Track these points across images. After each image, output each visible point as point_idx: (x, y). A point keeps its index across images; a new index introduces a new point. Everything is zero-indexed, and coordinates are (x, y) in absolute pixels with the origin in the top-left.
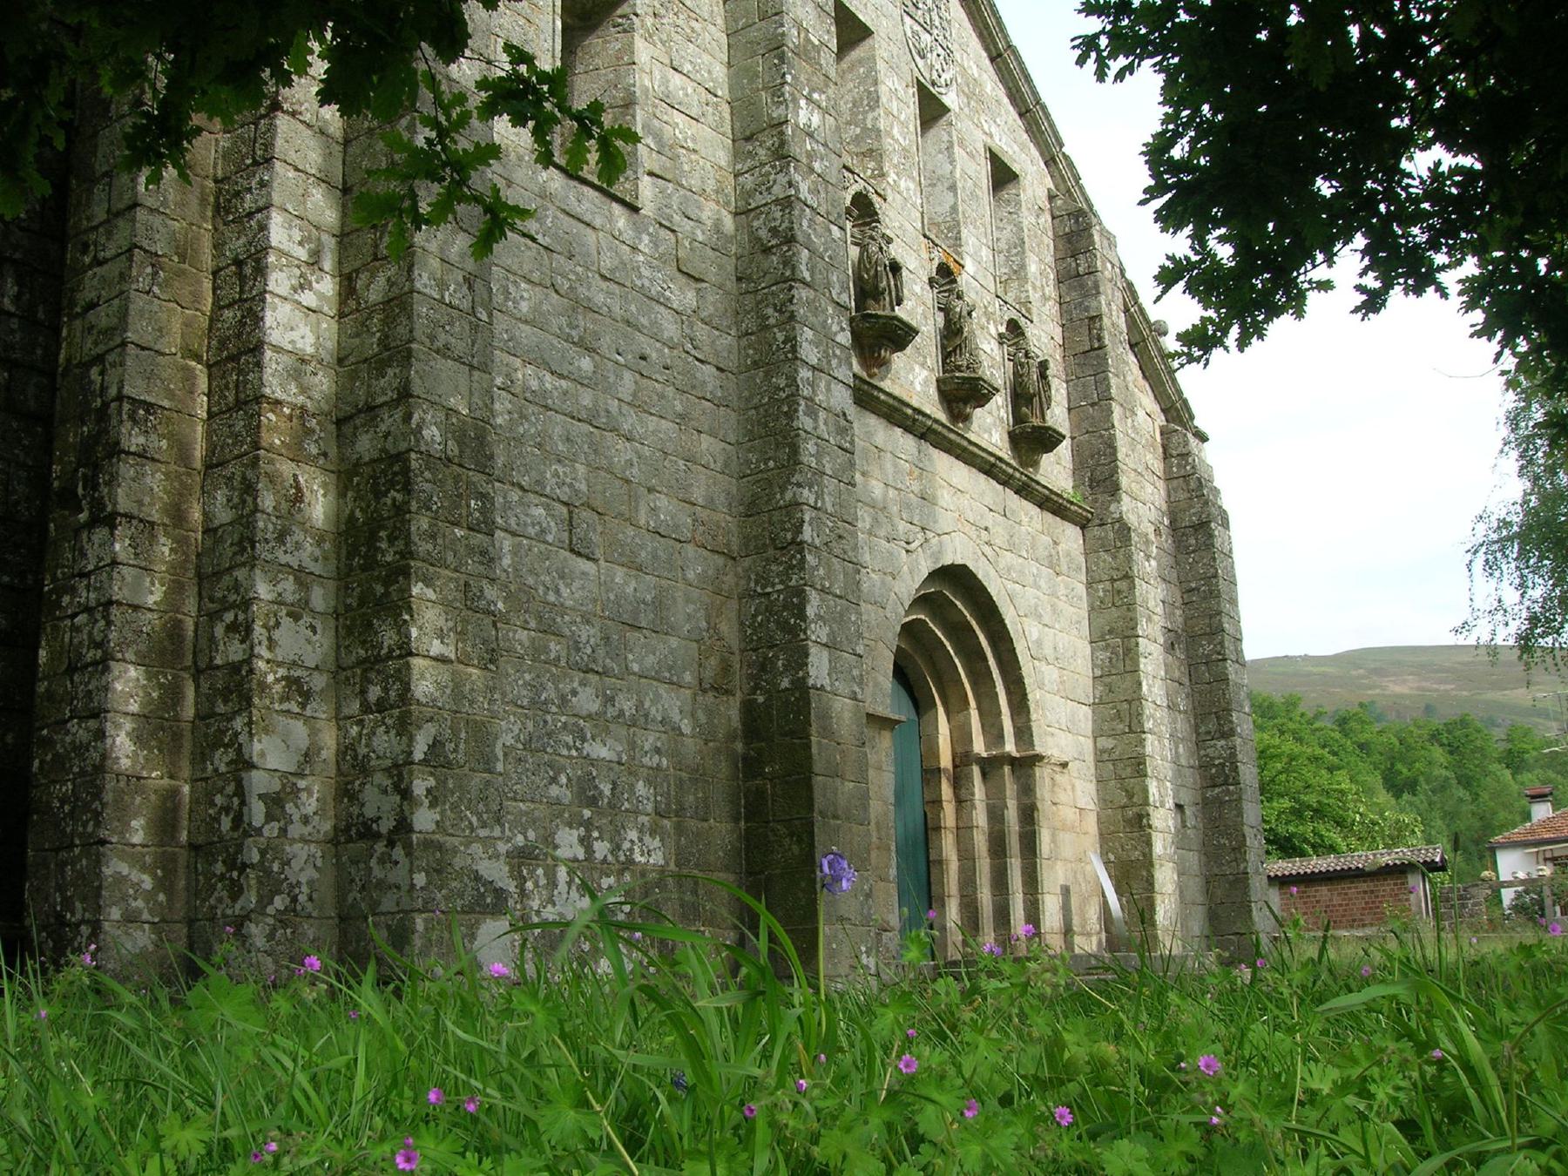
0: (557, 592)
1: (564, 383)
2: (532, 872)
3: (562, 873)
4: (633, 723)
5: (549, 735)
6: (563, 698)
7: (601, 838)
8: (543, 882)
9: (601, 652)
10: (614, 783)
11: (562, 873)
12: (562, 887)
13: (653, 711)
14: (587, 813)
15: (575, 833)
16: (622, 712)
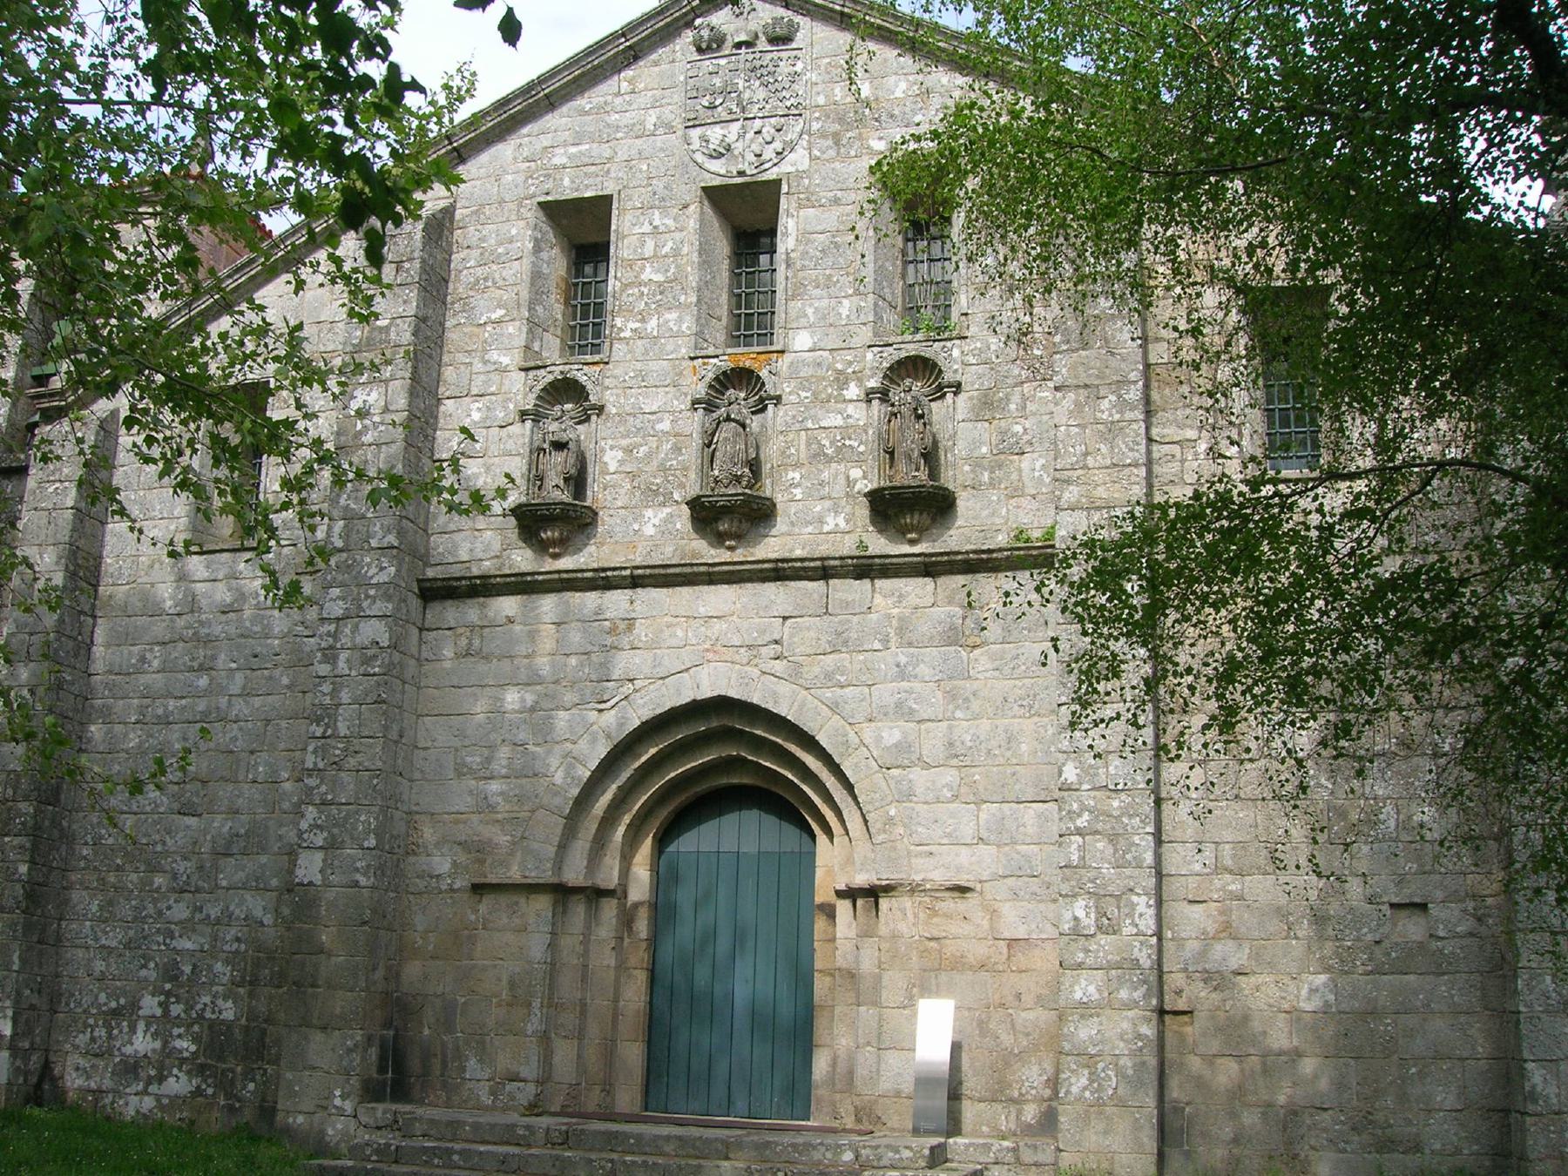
0: (164, 843)
1: (184, 702)
2: (118, 1025)
4: (218, 922)
5: (145, 938)
6: (160, 913)
7: (178, 1002)
8: (126, 1030)
9: (194, 878)
10: (195, 966)
11: (141, 1026)
12: (140, 1034)
13: (237, 912)
14: (168, 986)
15: (156, 999)
16: (208, 916)
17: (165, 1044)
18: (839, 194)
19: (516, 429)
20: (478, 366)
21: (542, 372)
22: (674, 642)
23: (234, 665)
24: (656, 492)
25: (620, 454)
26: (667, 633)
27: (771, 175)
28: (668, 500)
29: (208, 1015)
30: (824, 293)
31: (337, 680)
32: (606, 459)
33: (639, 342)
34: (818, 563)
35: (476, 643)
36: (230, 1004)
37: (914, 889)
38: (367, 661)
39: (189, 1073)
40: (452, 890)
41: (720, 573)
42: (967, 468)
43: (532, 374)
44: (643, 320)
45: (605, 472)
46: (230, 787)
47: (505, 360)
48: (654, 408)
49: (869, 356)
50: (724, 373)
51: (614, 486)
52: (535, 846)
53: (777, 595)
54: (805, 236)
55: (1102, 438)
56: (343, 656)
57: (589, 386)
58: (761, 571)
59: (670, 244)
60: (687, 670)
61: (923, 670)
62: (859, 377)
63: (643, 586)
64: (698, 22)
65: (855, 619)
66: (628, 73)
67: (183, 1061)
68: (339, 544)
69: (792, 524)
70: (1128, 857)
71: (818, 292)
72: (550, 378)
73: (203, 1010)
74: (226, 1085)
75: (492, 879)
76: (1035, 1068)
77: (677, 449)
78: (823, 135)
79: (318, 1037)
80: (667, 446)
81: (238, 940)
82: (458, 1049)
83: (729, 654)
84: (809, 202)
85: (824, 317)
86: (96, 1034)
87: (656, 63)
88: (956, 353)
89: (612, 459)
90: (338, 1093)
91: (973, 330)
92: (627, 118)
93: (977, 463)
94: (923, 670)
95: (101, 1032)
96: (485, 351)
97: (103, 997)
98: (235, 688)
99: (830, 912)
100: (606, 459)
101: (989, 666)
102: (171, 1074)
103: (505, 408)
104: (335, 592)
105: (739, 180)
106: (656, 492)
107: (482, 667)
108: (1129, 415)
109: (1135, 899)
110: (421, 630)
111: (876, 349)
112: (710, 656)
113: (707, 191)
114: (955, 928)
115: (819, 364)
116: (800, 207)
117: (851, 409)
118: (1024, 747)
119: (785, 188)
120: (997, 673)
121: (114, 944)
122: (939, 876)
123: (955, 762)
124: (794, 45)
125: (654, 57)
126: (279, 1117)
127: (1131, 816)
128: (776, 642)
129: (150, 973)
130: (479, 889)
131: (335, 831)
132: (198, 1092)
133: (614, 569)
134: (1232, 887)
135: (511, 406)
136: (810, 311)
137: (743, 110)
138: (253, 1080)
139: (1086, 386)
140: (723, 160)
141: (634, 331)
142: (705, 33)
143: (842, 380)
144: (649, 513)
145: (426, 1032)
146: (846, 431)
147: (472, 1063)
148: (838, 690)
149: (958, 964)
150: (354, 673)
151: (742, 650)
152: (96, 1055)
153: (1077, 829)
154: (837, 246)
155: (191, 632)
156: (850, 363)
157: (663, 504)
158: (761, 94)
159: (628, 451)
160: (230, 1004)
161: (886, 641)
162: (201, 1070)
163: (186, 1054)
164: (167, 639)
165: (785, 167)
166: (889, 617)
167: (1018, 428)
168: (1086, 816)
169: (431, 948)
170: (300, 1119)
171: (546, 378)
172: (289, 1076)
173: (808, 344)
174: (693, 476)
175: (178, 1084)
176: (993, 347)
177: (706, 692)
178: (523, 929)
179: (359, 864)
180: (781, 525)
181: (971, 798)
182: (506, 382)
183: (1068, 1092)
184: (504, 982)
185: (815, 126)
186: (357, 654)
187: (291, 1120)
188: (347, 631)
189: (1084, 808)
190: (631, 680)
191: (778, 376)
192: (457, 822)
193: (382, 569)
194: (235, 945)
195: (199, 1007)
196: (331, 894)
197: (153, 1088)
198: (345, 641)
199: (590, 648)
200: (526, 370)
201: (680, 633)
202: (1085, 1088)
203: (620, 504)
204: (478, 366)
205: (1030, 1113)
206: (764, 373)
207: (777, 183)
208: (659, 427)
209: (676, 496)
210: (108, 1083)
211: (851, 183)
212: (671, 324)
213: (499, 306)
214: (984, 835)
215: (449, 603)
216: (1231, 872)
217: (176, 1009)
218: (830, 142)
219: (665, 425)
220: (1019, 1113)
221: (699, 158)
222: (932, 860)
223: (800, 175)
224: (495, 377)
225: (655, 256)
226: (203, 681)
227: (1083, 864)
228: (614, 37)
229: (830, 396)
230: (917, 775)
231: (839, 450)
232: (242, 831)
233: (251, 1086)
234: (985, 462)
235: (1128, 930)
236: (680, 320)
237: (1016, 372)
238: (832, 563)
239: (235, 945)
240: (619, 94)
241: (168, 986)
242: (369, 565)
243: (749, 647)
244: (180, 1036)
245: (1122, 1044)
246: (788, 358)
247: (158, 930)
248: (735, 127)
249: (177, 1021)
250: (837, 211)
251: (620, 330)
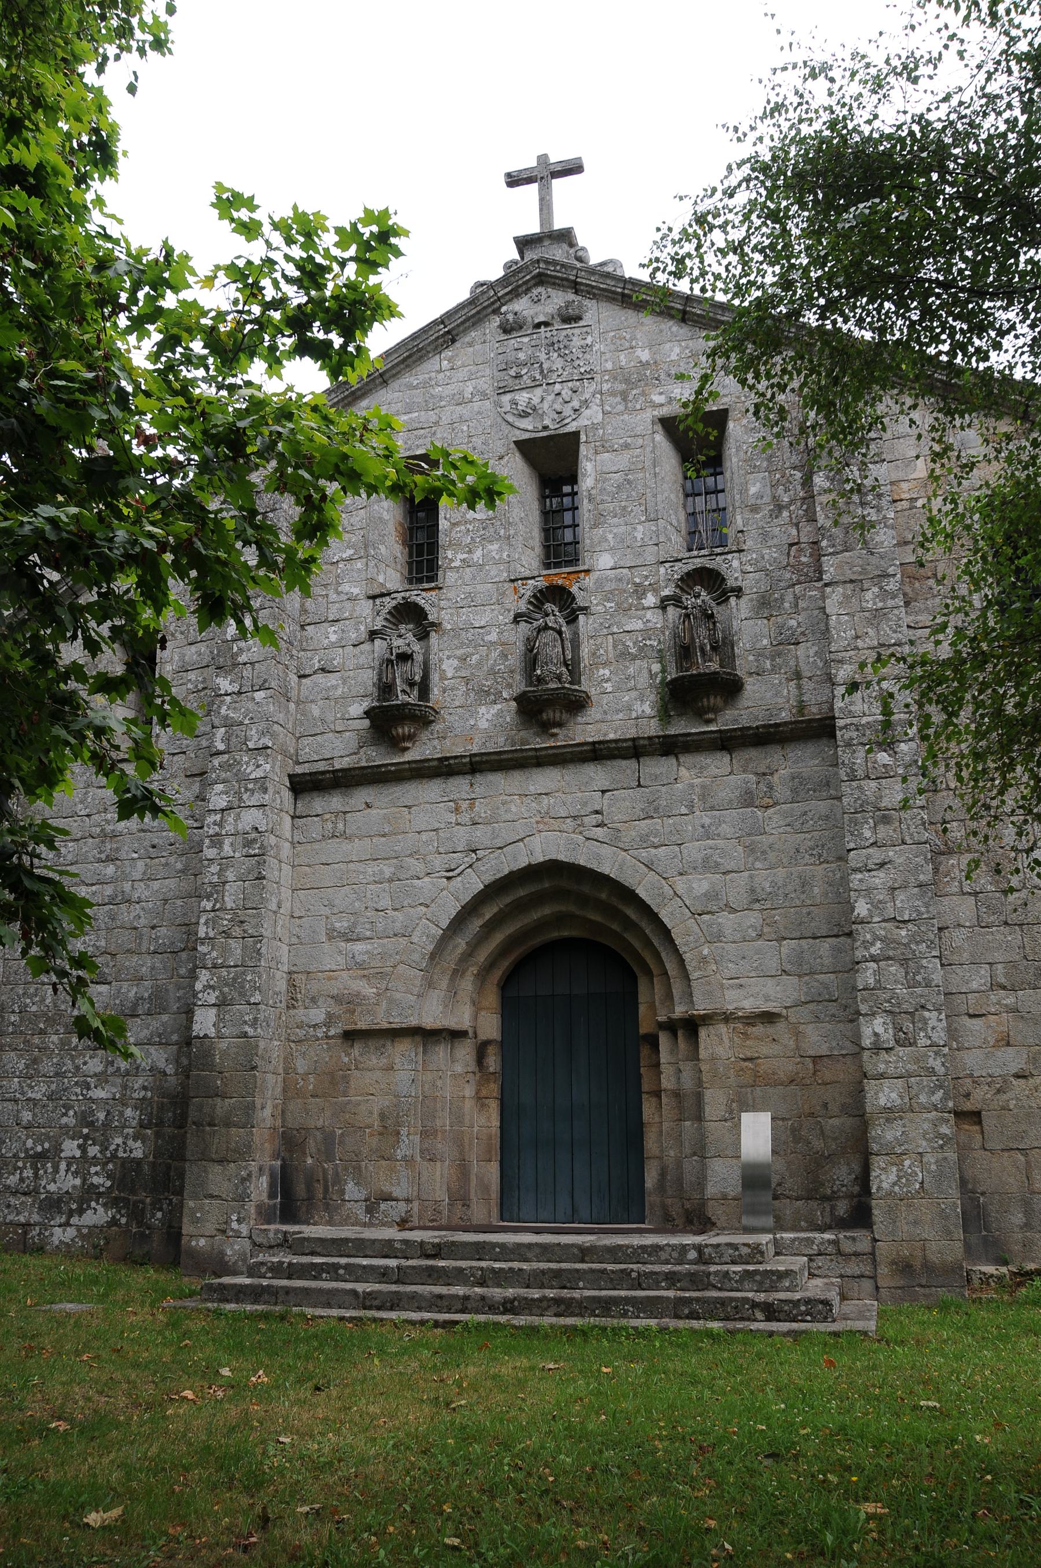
1: (94, 888)
2: (44, 1166)
3: (63, 1166)
4: (127, 1073)
5: (65, 1090)
6: (77, 1068)
7: (94, 1144)
8: (50, 1170)
10: (108, 1113)
11: (63, 1166)
12: (62, 1173)
13: (144, 1064)
14: (85, 1131)
15: (76, 1143)
16: (119, 1069)
17: (84, 1180)
18: (629, 440)
19: (366, 647)
20: (333, 597)
21: (387, 599)
22: (509, 817)
23: (135, 856)
24: (488, 693)
25: (456, 662)
26: (503, 809)
27: (572, 428)
28: (498, 698)
29: (121, 1154)
30: (621, 521)
31: (224, 863)
32: (444, 667)
33: (468, 570)
34: (630, 743)
35: (341, 826)
36: (139, 1144)
37: (727, 1018)
38: (248, 844)
39: (105, 1205)
40: (327, 1037)
41: (546, 756)
42: (751, 658)
43: (378, 601)
44: (470, 552)
45: (443, 678)
46: (135, 958)
47: (356, 591)
48: (482, 623)
49: (662, 570)
50: (541, 591)
51: (452, 689)
52: (398, 996)
53: (597, 775)
54: (602, 476)
55: (869, 622)
56: (227, 842)
57: (427, 608)
58: (581, 752)
60: (522, 840)
61: (725, 829)
62: (654, 588)
63: (481, 771)
64: (504, 309)
65: (664, 789)
66: (447, 353)
67: (100, 1195)
68: (221, 747)
69: (605, 713)
70: (918, 978)
71: (616, 520)
72: (394, 602)
73: (116, 1150)
74: (137, 1214)
75: (362, 1025)
76: (844, 1169)
77: (504, 656)
78: (613, 393)
79: (218, 1168)
80: (494, 654)
81: (145, 1088)
82: (337, 1174)
83: (556, 824)
84: (604, 447)
85: (622, 541)
86: (25, 1175)
87: (470, 344)
88: (735, 564)
89: (449, 667)
90: (234, 1217)
91: (749, 543)
92: (450, 390)
93: (760, 654)
94: (725, 829)
95: (28, 1173)
96: (339, 584)
97: (30, 1143)
98: (137, 876)
99: (653, 1042)
100: (444, 667)
101: (781, 823)
102: (89, 1207)
103: (357, 630)
104: (219, 787)
105: (545, 434)
106: (488, 693)
107: (346, 846)
108: (890, 603)
109: (927, 1014)
110: (293, 818)
111: (667, 565)
112: (541, 826)
113: (520, 445)
114: (765, 1050)
115: (620, 580)
116: (596, 453)
117: (649, 614)
118: (816, 890)
119: (583, 438)
120: (788, 829)
121: (39, 1096)
122: (749, 1005)
123: (757, 906)
124: (581, 323)
125: (467, 339)
126: (184, 1240)
127: (917, 943)
128: (597, 812)
129: (69, 1120)
130: (350, 1036)
131: (226, 989)
132: (114, 1222)
133: (456, 757)
134: (1008, 1001)
135: (362, 628)
136: (610, 536)
137: (544, 377)
138: (160, 1209)
139: (852, 581)
140: (530, 418)
141: (463, 560)
142: (510, 317)
143: (640, 592)
144: (482, 710)
145: (309, 1161)
146: (647, 633)
147: (350, 1186)
148: (653, 850)
149: (770, 1081)
150: (237, 855)
151: (568, 820)
152: (25, 1194)
153: (872, 956)
154: (629, 482)
155: (98, 830)
156: (647, 577)
157: (495, 702)
158: (559, 363)
159: (463, 659)
160: (139, 1144)
161: (691, 807)
162: (112, 1203)
163: (102, 1189)
164: (79, 836)
165: (583, 422)
166: (692, 786)
167: (793, 623)
168: (878, 945)
169: (311, 1087)
170: (202, 1242)
171: (389, 603)
172: (191, 1204)
173: (611, 564)
174: (518, 677)
175: (97, 1215)
176: (767, 557)
177: (539, 858)
178: (390, 1068)
179: (247, 1018)
180: (593, 713)
181: (773, 936)
182: (357, 608)
183: (879, 1188)
184: (376, 1116)
185: (606, 387)
186: (239, 839)
187: (193, 1243)
188: (231, 820)
189: (876, 938)
190: (474, 851)
191: (583, 591)
192: (330, 979)
193: (258, 766)
194: (143, 1093)
195: (113, 1147)
196: (223, 1045)
197: (74, 1220)
198: (229, 828)
199: (437, 825)
200: (373, 597)
201: (514, 809)
202: (895, 1184)
203: (457, 704)
204: (333, 597)
205: (842, 1208)
206: (574, 589)
207: (576, 434)
208: (487, 638)
209: (505, 695)
210: (35, 1218)
211: (639, 430)
212: (494, 554)
213: (348, 547)
214: (788, 967)
215: (315, 794)
216: (1004, 988)
217: (93, 1151)
218: (618, 399)
219: (493, 637)
220: (833, 1208)
221: (510, 418)
222: (742, 992)
223: (595, 427)
224: (348, 605)
226: (110, 870)
227: (879, 986)
228: (435, 323)
229: (631, 605)
230: (725, 920)
231: (641, 649)
232: (146, 995)
233: (159, 1215)
234: (767, 653)
235: (923, 1041)
236: (501, 550)
237: (788, 575)
238: (642, 742)
239: (143, 1093)
240: (441, 371)
241: (85, 1131)
242: (247, 763)
243: (575, 818)
244: (96, 1173)
245: (924, 1143)
246: (594, 576)
247: (76, 1083)
248: (539, 392)
249: (95, 1160)
250: (626, 455)
251: (452, 561)
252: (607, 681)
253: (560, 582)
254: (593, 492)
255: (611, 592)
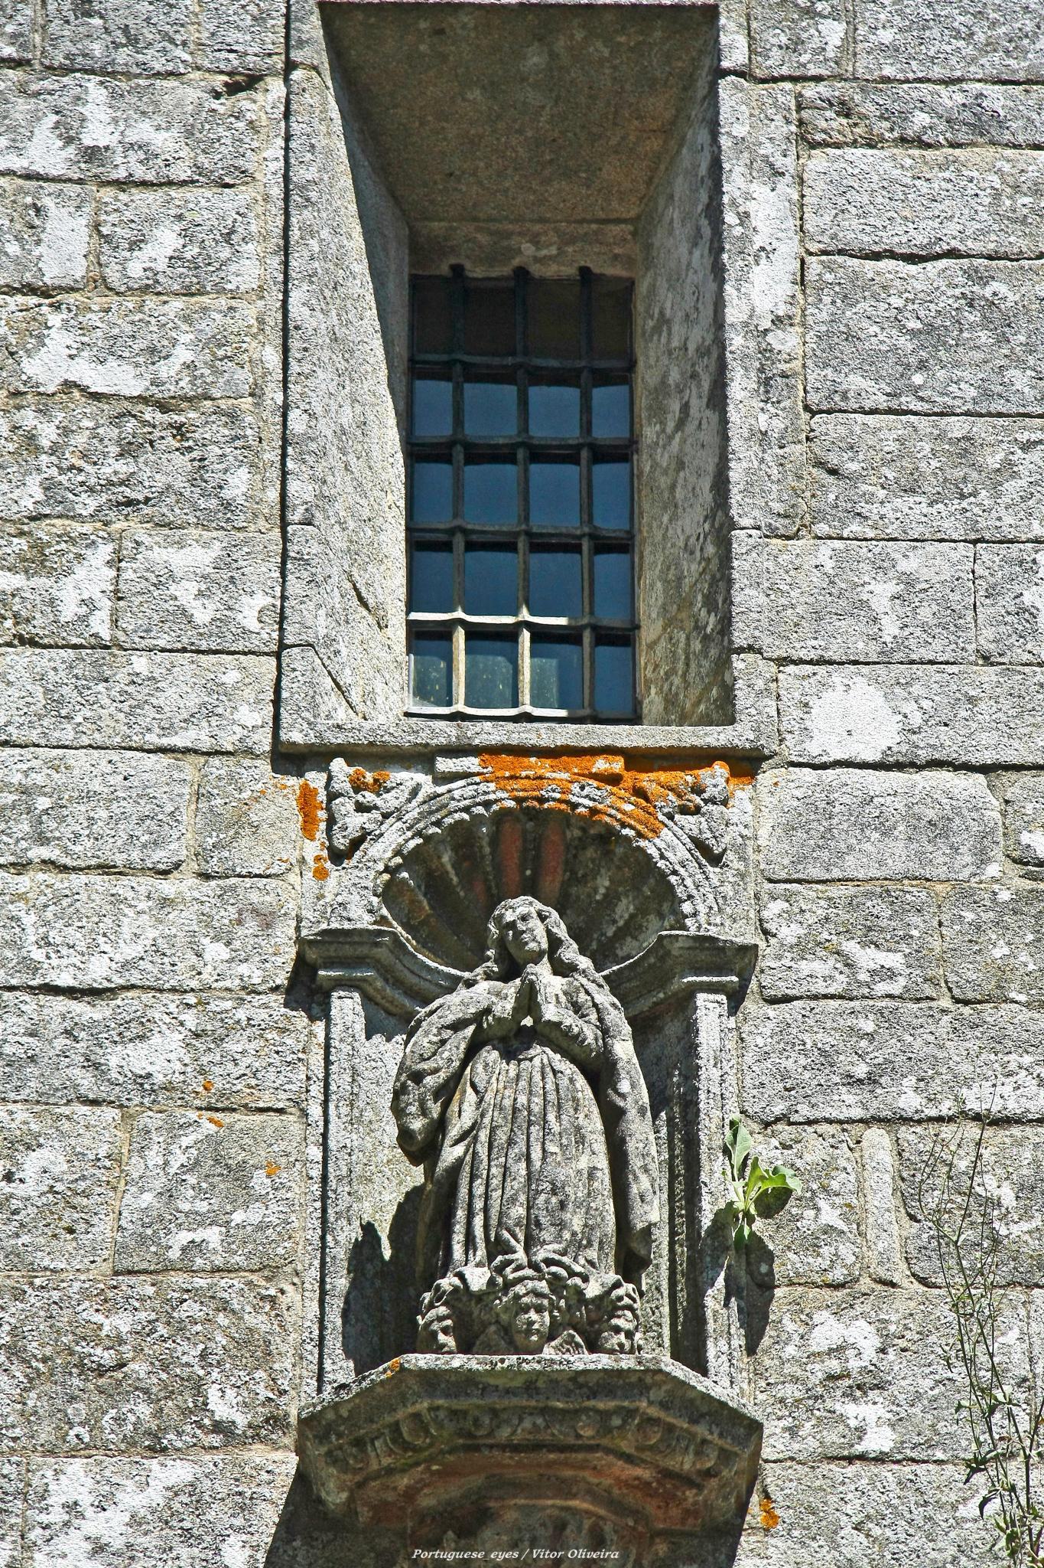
18: (997, 98)
48: (98, 972)
50: (462, 836)
59: (166, 241)
71: (912, 509)
85: (951, 620)
115: (940, 829)
116: (806, 140)
136: (881, 592)
174: (299, 1304)
212: (185, 592)
225: (99, 283)
229: (1002, 972)
252: (860, 1388)
253: (585, 796)
254: (786, 341)
255: (887, 887)
